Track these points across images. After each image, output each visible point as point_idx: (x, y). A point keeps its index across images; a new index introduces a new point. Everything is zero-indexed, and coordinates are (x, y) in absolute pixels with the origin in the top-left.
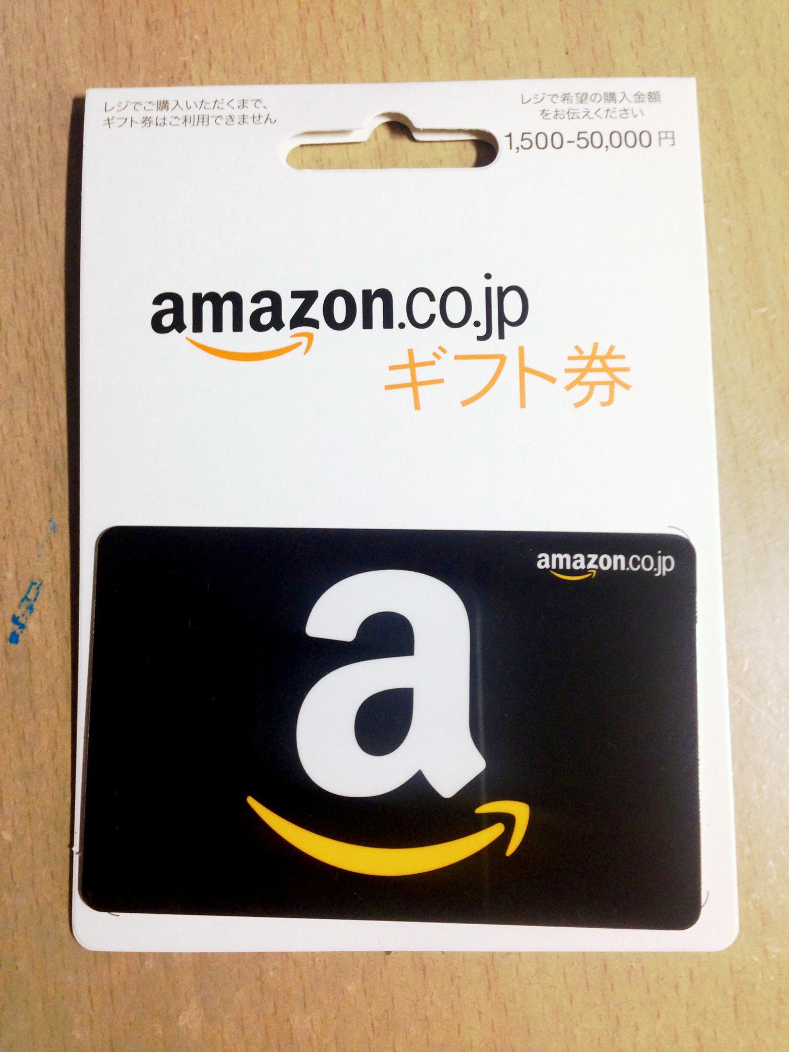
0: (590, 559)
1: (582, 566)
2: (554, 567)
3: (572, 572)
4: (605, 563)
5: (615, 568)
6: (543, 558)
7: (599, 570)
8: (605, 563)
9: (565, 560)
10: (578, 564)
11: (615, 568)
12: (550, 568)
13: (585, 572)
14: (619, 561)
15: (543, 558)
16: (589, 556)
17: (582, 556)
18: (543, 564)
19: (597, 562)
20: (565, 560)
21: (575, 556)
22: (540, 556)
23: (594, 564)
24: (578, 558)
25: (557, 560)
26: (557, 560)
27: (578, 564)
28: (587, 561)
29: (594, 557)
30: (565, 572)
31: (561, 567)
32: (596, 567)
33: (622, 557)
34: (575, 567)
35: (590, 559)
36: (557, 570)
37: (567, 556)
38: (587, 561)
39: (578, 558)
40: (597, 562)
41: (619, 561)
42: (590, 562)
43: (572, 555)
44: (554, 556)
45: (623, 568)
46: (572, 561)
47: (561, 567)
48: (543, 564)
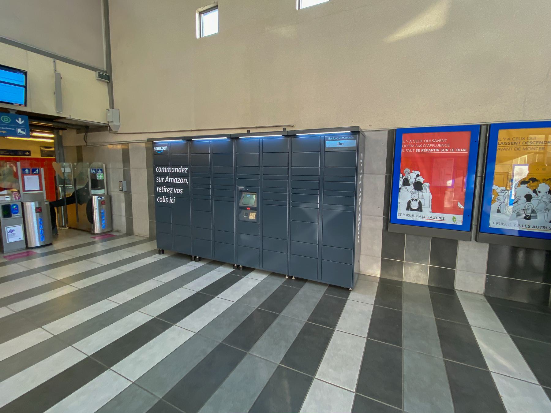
1: (161, 150)
7: (163, 150)
13: (161, 151)
28: (161, 148)
29: (162, 147)
36: (157, 151)
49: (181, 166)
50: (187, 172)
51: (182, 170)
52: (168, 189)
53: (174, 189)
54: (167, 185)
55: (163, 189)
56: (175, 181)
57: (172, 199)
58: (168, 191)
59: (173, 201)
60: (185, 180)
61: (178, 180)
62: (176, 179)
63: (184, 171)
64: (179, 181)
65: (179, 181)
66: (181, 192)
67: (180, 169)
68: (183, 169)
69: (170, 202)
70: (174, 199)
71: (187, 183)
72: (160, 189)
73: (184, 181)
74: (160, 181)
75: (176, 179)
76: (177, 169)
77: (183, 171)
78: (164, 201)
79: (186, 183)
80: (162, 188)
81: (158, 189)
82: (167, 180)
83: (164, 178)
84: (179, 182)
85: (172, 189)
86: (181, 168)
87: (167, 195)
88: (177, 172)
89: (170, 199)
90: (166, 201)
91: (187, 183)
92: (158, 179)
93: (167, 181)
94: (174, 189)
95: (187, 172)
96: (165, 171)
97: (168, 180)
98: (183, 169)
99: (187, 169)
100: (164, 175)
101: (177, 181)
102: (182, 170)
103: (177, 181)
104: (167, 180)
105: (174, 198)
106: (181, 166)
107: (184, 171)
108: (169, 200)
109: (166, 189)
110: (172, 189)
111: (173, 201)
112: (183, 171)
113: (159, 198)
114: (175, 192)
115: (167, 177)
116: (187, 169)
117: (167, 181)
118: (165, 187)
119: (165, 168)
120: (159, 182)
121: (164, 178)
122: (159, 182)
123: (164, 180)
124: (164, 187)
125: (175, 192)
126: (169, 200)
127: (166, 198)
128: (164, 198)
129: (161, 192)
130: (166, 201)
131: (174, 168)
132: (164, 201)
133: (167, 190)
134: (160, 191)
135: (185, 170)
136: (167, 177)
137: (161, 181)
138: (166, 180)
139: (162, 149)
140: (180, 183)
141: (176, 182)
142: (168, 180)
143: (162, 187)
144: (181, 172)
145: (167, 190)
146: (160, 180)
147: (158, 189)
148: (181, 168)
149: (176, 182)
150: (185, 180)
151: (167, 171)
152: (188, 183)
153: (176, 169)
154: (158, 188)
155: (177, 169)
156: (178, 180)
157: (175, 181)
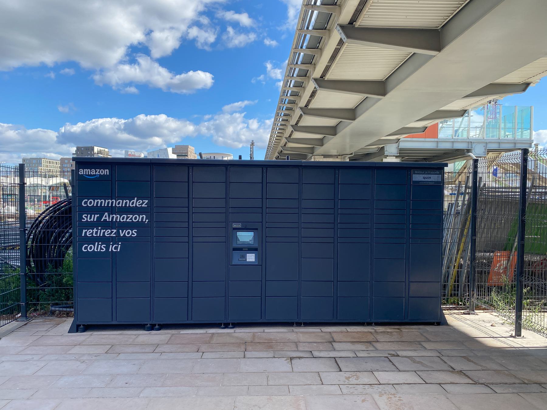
2: (85, 174)
3: (91, 175)
4: (102, 173)
5: (105, 174)
8: (102, 173)
9: (88, 171)
10: (93, 173)
11: (105, 174)
12: (84, 174)
14: (107, 171)
17: (94, 170)
18: (81, 173)
19: (99, 172)
20: (88, 171)
22: (80, 170)
23: (98, 172)
25: (86, 171)
26: (86, 171)
27: (93, 173)
28: (96, 172)
29: (98, 170)
30: (88, 175)
31: (87, 174)
32: (99, 174)
33: (108, 170)
34: (92, 174)
36: (86, 175)
37: (89, 170)
38: (96, 172)
40: (99, 172)
41: (107, 171)
45: (108, 174)
46: (91, 171)
47: (87, 174)
48: (81, 173)
49: (136, 198)
50: (146, 206)
51: (136, 203)
52: (108, 231)
53: (121, 231)
54: (107, 225)
55: (96, 233)
56: (123, 218)
57: (115, 245)
58: (107, 234)
59: (116, 248)
60: (143, 218)
61: (127, 218)
62: (126, 216)
63: (142, 204)
64: (131, 219)
65: (131, 219)
66: (132, 234)
67: (134, 202)
68: (140, 202)
69: (110, 250)
70: (119, 246)
71: (146, 220)
72: (90, 231)
73: (143, 218)
74: (89, 220)
75: (124, 217)
76: (126, 203)
77: (139, 205)
78: (97, 249)
79: (144, 221)
80: (95, 230)
81: (86, 233)
82: (106, 217)
83: (98, 215)
84: (131, 221)
85: (115, 231)
86: (135, 201)
87: (104, 240)
88: (128, 206)
89: (111, 246)
90: (101, 249)
91: (145, 222)
92: (85, 216)
93: (105, 220)
94: (121, 231)
95: (146, 206)
96: (103, 205)
97: (107, 218)
98: (140, 202)
99: (147, 201)
100: (100, 210)
101: (127, 219)
102: (138, 204)
103: (127, 219)
104: (106, 217)
105: (120, 243)
106: (136, 198)
107: (142, 204)
108: (107, 248)
109: (102, 231)
110: (115, 231)
111: (116, 248)
112: (139, 205)
113: (87, 245)
114: (122, 235)
115: (106, 214)
116: (147, 201)
117: (105, 220)
118: (100, 228)
119: (103, 201)
120: (87, 221)
121: (98, 215)
122: (87, 221)
123: (99, 218)
124: (98, 229)
125: (122, 235)
126: (107, 248)
127: (101, 245)
128: (98, 245)
129: (93, 236)
130: (101, 249)
131: (121, 201)
132: (97, 249)
133: (104, 233)
134: (89, 234)
135: (143, 203)
136: (106, 214)
137: (92, 220)
138: (104, 218)
140: (133, 221)
141: (125, 220)
142: (106, 217)
143: (93, 229)
144: (134, 205)
145: (104, 233)
146: (90, 218)
147: (86, 233)
148: (135, 201)
149: (125, 220)
150: (143, 218)
151: (106, 205)
152: (147, 221)
153: (124, 201)
154: (84, 231)
155: (126, 203)
156: (127, 218)
157: (123, 218)
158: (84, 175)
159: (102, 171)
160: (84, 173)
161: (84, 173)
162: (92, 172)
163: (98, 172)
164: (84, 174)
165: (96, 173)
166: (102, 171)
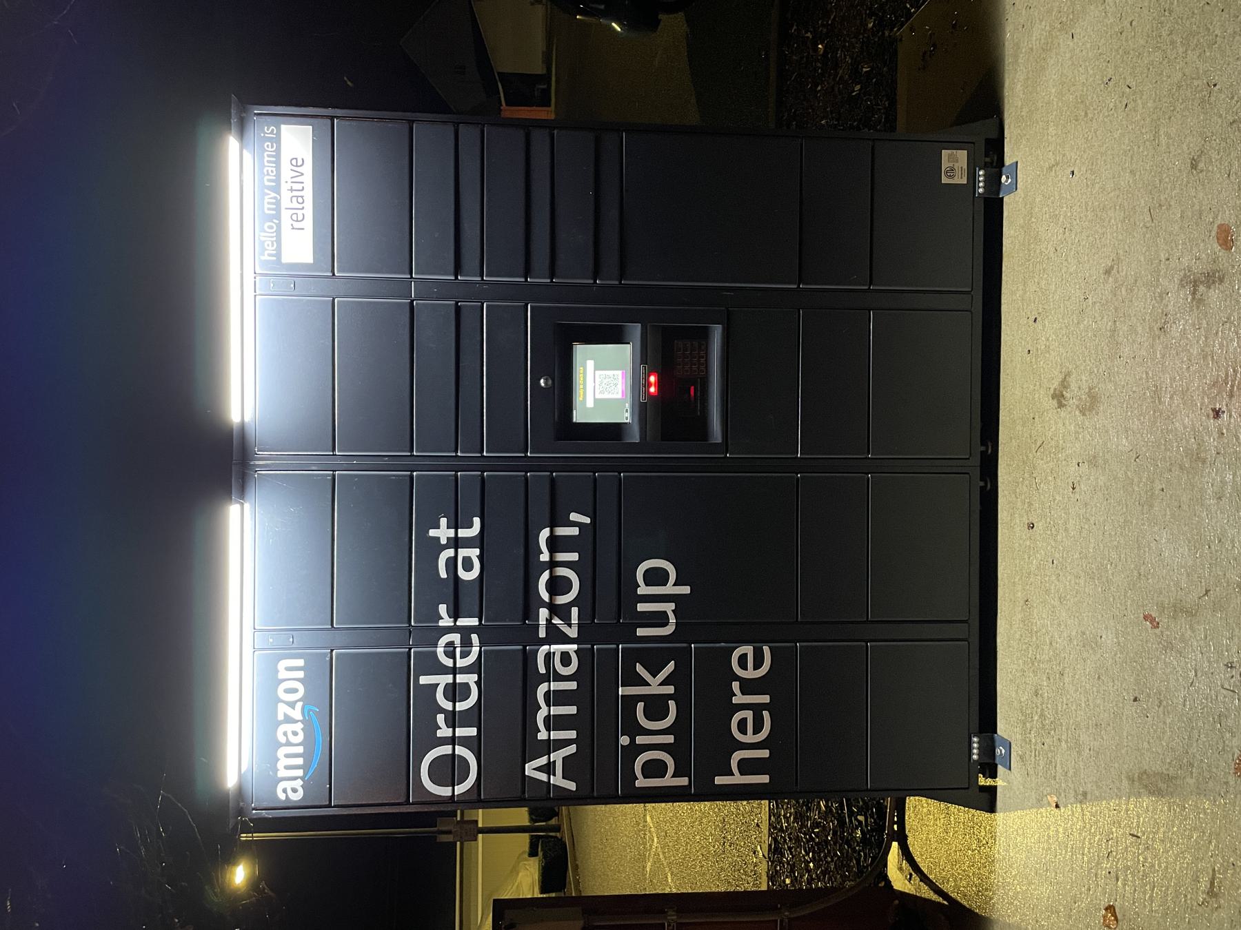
0: (285, 715)
1: (299, 727)
2: (300, 773)
4: (295, 691)
6: (285, 791)
8: (295, 691)
9: (287, 756)
10: (295, 734)
12: (302, 778)
15: (285, 791)
16: (281, 717)
19: (292, 705)
20: (287, 756)
21: (282, 739)
23: (294, 708)
24: (285, 734)
25: (287, 768)
26: (287, 768)
27: (295, 734)
28: (289, 720)
29: (282, 709)
32: (299, 705)
35: (285, 715)
37: (282, 752)
38: (289, 720)
39: (285, 734)
40: (292, 705)
42: (290, 714)
43: (282, 745)
44: (282, 773)
46: (289, 744)
47: (300, 761)
48: (294, 790)
139: (297, 714)
158: (305, 774)
159: (289, 691)
160: (295, 778)
161: (295, 778)
162: (294, 740)
163: (294, 708)
164: (302, 778)
165: (298, 721)
166: (289, 691)
